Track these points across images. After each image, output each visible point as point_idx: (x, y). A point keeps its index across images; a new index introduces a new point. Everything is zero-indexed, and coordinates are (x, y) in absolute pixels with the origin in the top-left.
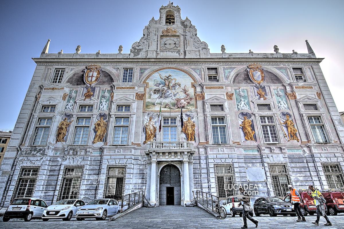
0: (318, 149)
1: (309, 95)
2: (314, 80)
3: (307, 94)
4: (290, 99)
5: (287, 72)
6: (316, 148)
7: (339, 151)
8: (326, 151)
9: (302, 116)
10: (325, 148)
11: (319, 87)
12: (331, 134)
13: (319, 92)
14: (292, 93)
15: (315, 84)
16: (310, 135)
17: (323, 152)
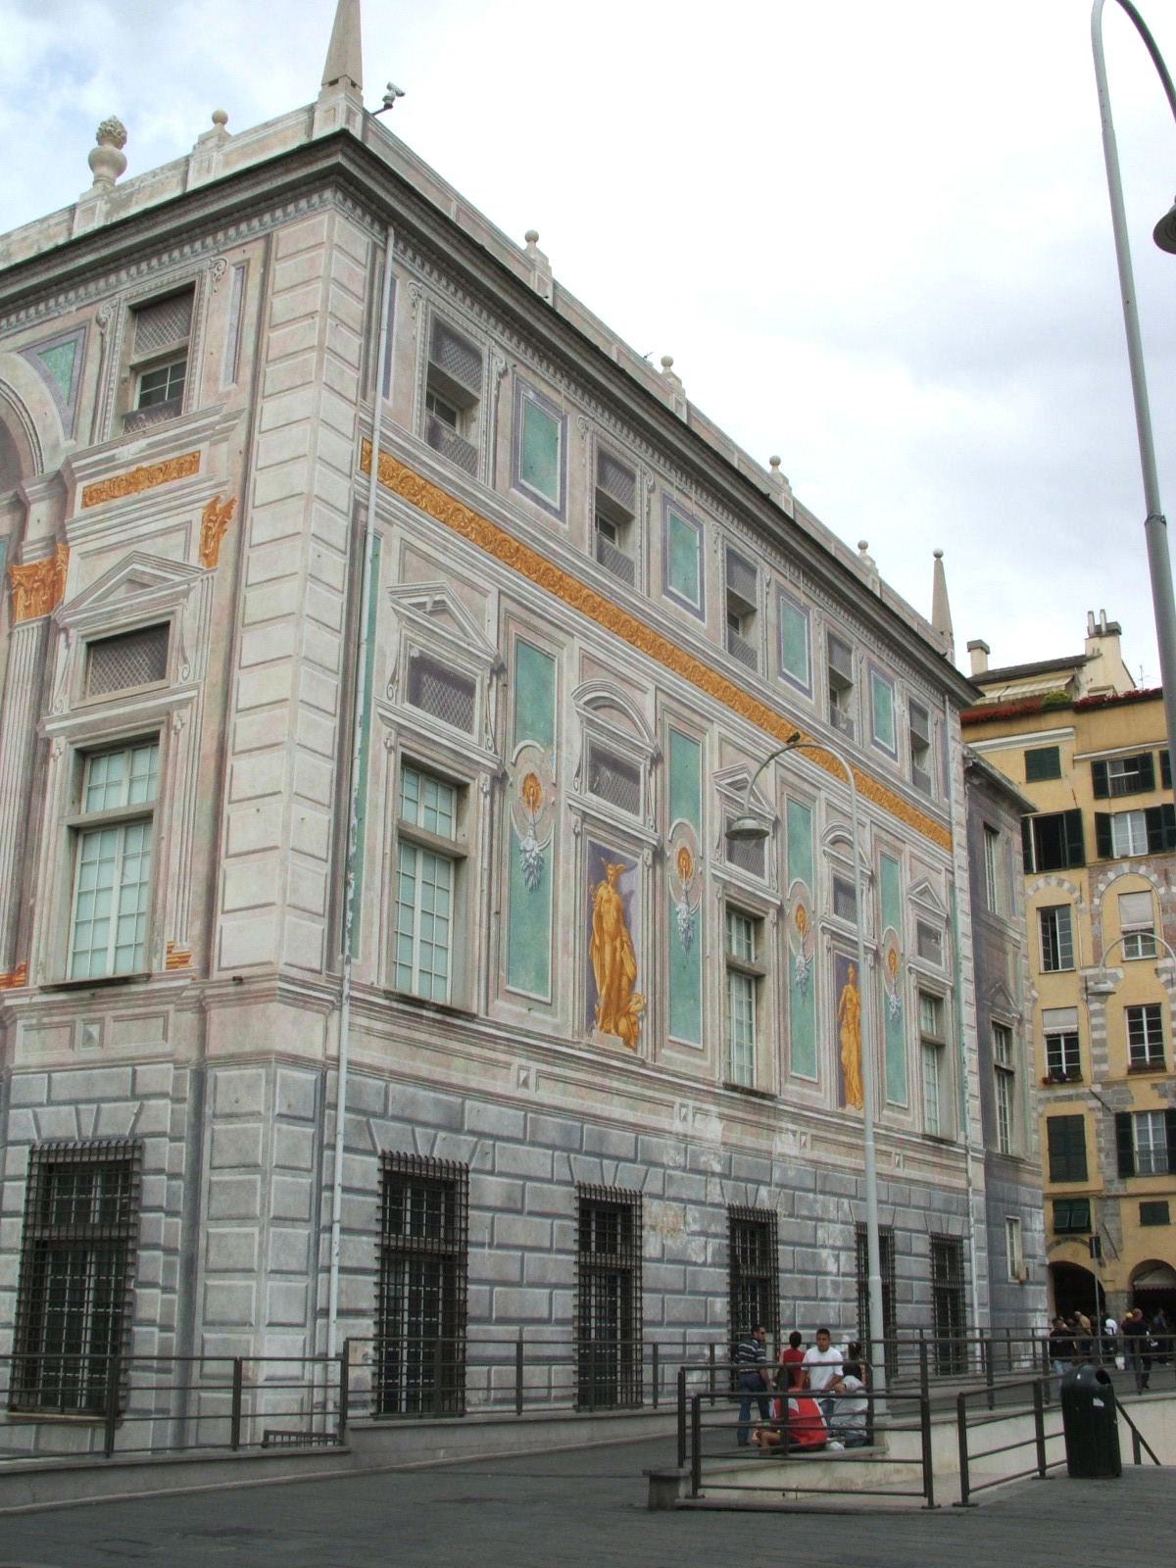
0: (51, 1035)
1: (145, 547)
2: (235, 380)
3: (140, 538)
4: (20, 620)
5: (82, 371)
6: (41, 1027)
7: (168, 1048)
8: (92, 1053)
9: (39, 761)
10: (92, 1021)
11: (242, 447)
12: (171, 896)
13: (231, 491)
14: (45, 560)
15: (227, 418)
16: (36, 918)
17: (70, 1056)
